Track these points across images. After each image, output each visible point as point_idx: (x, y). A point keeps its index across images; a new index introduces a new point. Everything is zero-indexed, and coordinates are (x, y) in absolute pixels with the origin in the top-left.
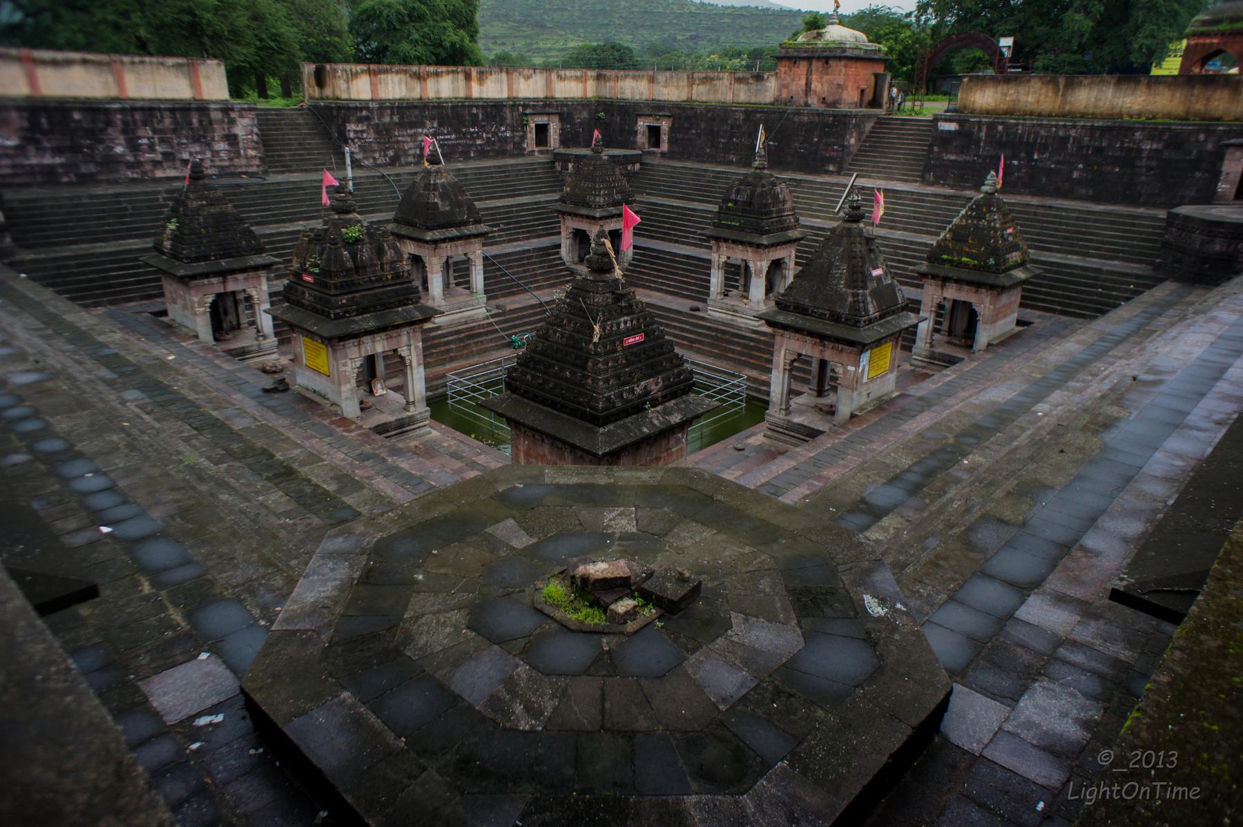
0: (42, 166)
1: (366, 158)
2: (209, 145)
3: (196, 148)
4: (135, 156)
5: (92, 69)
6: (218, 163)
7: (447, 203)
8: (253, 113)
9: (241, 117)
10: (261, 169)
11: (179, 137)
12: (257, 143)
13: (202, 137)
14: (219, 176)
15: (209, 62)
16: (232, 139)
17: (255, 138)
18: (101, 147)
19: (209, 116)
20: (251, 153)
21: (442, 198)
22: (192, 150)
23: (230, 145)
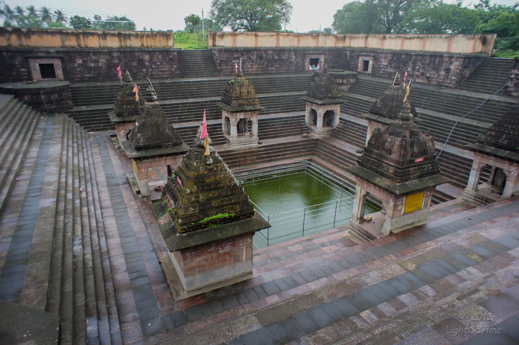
0: (389, 72)
1: (515, 91)
2: (438, 72)
3: (433, 72)
4: (413, 72)
5: (419, 40)
6: (438, 80)
7: (382, 103)
8: (463, 59)
9: (456, 61)
10: (454, 86)
11: (429, 67)
12: (458, 73)
13: (436, 69)
14: (436, 85)
15: (459, 35)
16: (448, 70)
17: (458, 71)
18: (405, 68)
19: (443, 59)
20: (453, 78)
21: (381, 101)
22: (431, 73)
23: (446, 73)
